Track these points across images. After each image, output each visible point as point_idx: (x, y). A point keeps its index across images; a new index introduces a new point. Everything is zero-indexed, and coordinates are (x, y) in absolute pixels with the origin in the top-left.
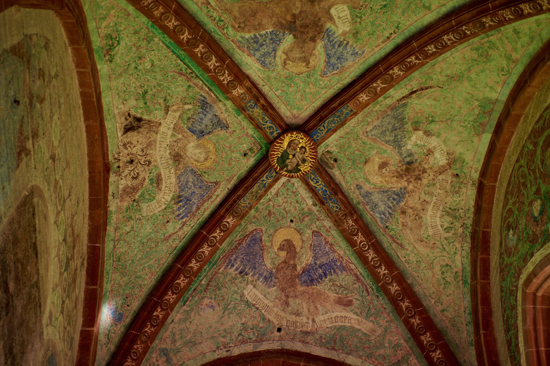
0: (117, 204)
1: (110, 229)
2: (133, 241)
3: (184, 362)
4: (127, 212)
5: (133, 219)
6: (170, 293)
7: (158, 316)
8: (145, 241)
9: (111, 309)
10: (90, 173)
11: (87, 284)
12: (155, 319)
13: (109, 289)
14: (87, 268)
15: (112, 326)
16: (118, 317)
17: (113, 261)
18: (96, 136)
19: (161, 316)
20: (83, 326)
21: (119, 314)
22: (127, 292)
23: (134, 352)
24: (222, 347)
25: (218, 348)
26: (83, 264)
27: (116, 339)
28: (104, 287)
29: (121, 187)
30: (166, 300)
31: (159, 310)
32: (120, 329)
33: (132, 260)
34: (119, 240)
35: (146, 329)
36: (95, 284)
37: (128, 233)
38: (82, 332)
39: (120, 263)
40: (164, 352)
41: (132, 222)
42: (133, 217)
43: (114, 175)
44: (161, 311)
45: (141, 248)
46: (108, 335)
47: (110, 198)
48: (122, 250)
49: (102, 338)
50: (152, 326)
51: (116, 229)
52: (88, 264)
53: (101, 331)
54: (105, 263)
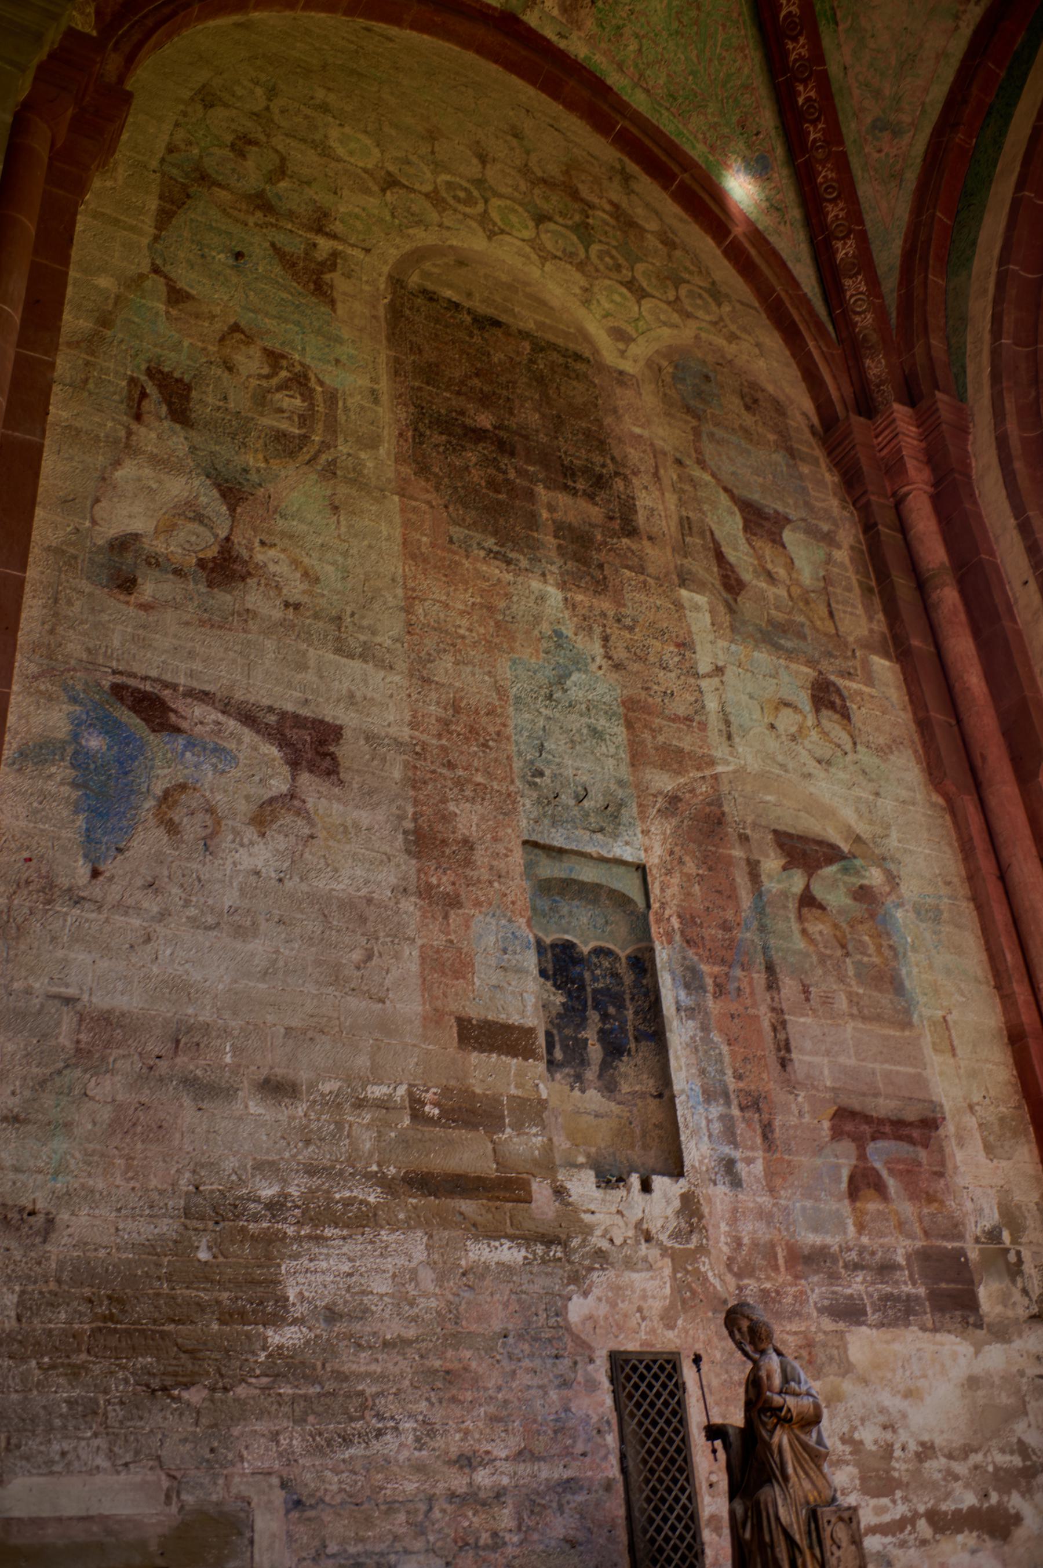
0: (580, 38)
1: (614, 79)
2: (660, 49)
3: (923, 104)
4: (604, 28)
5: (624, 25)
6: (790, 46)
7: (808, 99)
8: (675, 25)
9: (738, 171)
10: (496, 62)
11: (665, 188)
12: (809, 107)
13: (705, 149)
14: (643, 169)
15: (764, 188)
16: (759, 168)
17: (668, 109)
18: (438, 19)
19: (813, 94)
20: (719, 244)
21: (757, 161)
22: (734, 119)
23: (826, 189)
24: (962, 8)
25: (957, 17)
26: (627, 178)
27: (790, 197)
28: (696, 158)
29: (555, 12)
30: (795, 60)
31: (801, 88)
32: (782, 174)
33: (693, 73)
34: (641, 75)
35: (812, 137)
36: (674, 177)
37: (640, 50)
38: (726, 253)
39: (680, 100)
40: (879, 126)
41: (627, 31)
42: (621, 22)
43: (528, 12)
44: (806, 87)
45: (683, 41)
46: (772, 205)
47: (562, 44)
48: (661, 82)
49: (764, 223)
50: (814, 122)
51: (620, 67)
52: (638, 162)
53: (753, 217)
54: (662, 127)
